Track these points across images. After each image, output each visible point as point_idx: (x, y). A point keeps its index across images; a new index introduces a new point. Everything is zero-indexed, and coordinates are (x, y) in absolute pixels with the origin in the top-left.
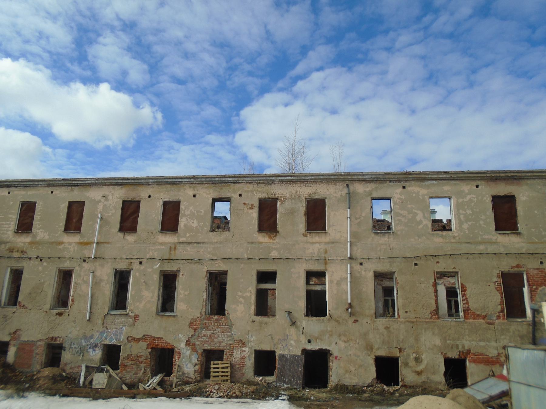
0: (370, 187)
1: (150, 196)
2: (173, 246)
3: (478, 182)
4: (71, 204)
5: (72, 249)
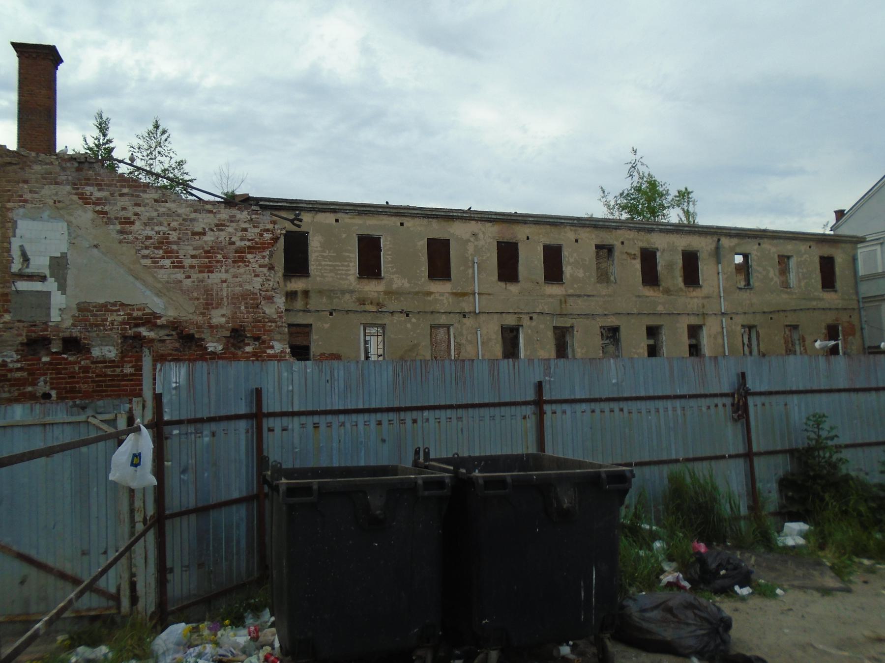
0: (735, 241)
1: (528, 238)
2: (563, 299)
3: (811, 243)
4: (431, 242)
5: (445, 301)
